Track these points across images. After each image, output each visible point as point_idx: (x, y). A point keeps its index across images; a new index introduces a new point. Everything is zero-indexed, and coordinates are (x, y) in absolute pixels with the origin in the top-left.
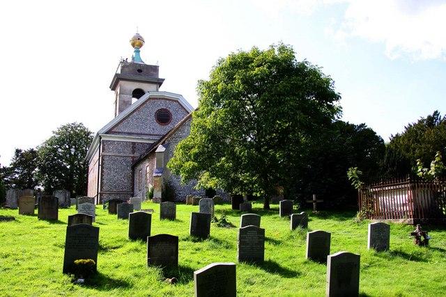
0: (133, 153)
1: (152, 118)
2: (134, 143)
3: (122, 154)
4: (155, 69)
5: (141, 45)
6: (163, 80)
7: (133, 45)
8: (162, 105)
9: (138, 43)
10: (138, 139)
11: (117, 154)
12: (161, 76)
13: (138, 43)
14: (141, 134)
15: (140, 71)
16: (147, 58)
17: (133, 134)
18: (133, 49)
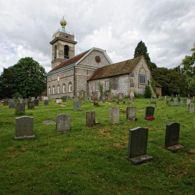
0: (87, 74)
1: (94, 60)
2: (87, 70)
3: (83, 75)
4: (73, 36)
5: (65, 25)
6: (77, 42)
7: (62, 25)
8: (97, 54)
9: (63, 24)
10: (89, 68)
11: (81, 75)
12: (75, 40)
13: (63, 24)
14: (90, 66)
15: (67, 37)
16: (68, 30)
17: (87, 66)
18: (62, 27)
